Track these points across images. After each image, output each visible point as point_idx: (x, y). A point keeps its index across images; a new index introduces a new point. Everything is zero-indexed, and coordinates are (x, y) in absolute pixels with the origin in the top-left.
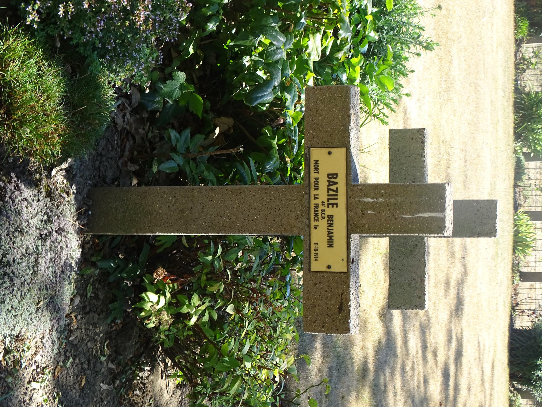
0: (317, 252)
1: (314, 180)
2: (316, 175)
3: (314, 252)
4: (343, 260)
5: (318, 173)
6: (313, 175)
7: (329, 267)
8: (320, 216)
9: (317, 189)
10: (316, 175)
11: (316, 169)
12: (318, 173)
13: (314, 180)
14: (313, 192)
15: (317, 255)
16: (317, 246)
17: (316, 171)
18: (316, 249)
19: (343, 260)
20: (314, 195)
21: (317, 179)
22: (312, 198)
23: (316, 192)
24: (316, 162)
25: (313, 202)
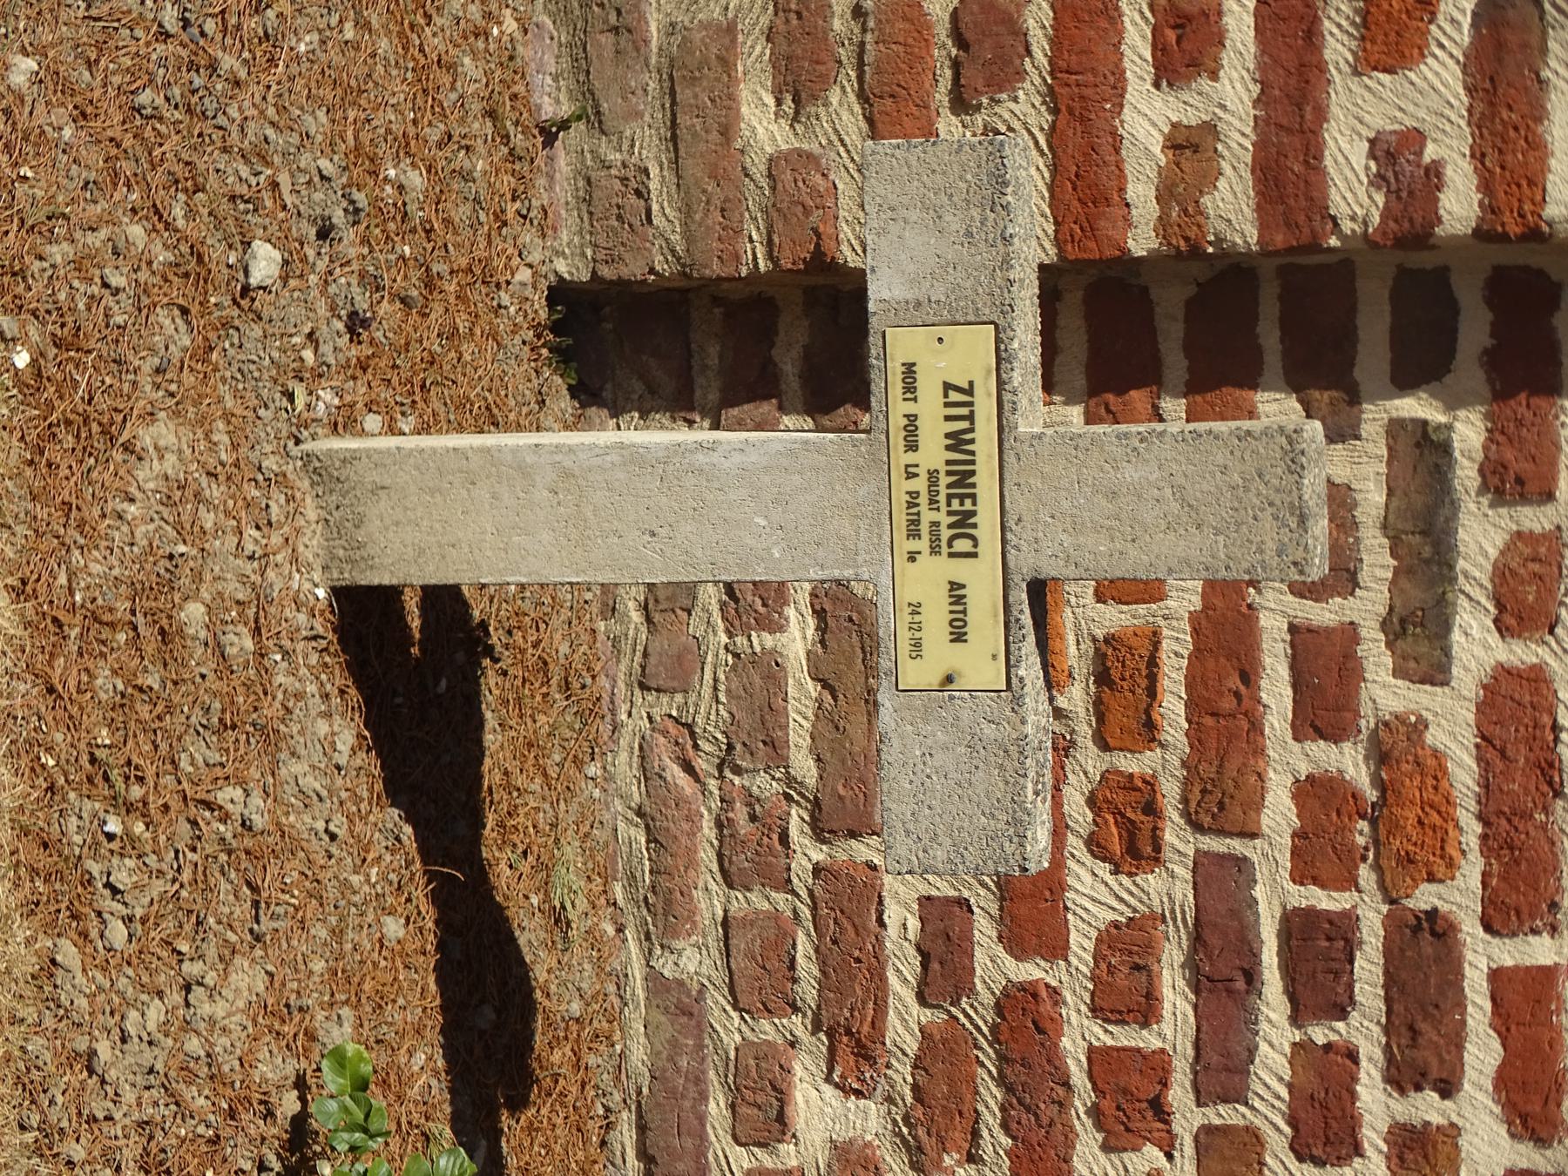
0: (918, 635)
1: (905, 422)
2: (910, 408)
3: (909, 635)
4: (994, 657)
5: (915, 400)
6: (899, 408)
7: (949, 679)
8: (924, 528)
9: (912, 446)
10: (910, 408)
11: (910, 388)
12: (915, 400)
13: (905, 422)
14: (902, 458)
15: (917, 645)
16: (917, 618)
17: (908, 395)
18: (916, 627)
19: (994, 657)
20: (907, 466)
21: (912, 418)
22: (897, 474)
23: (911, 458)
24: (910, 369)
25: (902, 487)
